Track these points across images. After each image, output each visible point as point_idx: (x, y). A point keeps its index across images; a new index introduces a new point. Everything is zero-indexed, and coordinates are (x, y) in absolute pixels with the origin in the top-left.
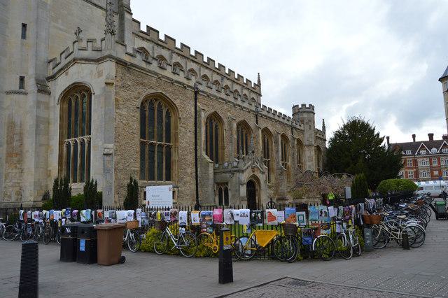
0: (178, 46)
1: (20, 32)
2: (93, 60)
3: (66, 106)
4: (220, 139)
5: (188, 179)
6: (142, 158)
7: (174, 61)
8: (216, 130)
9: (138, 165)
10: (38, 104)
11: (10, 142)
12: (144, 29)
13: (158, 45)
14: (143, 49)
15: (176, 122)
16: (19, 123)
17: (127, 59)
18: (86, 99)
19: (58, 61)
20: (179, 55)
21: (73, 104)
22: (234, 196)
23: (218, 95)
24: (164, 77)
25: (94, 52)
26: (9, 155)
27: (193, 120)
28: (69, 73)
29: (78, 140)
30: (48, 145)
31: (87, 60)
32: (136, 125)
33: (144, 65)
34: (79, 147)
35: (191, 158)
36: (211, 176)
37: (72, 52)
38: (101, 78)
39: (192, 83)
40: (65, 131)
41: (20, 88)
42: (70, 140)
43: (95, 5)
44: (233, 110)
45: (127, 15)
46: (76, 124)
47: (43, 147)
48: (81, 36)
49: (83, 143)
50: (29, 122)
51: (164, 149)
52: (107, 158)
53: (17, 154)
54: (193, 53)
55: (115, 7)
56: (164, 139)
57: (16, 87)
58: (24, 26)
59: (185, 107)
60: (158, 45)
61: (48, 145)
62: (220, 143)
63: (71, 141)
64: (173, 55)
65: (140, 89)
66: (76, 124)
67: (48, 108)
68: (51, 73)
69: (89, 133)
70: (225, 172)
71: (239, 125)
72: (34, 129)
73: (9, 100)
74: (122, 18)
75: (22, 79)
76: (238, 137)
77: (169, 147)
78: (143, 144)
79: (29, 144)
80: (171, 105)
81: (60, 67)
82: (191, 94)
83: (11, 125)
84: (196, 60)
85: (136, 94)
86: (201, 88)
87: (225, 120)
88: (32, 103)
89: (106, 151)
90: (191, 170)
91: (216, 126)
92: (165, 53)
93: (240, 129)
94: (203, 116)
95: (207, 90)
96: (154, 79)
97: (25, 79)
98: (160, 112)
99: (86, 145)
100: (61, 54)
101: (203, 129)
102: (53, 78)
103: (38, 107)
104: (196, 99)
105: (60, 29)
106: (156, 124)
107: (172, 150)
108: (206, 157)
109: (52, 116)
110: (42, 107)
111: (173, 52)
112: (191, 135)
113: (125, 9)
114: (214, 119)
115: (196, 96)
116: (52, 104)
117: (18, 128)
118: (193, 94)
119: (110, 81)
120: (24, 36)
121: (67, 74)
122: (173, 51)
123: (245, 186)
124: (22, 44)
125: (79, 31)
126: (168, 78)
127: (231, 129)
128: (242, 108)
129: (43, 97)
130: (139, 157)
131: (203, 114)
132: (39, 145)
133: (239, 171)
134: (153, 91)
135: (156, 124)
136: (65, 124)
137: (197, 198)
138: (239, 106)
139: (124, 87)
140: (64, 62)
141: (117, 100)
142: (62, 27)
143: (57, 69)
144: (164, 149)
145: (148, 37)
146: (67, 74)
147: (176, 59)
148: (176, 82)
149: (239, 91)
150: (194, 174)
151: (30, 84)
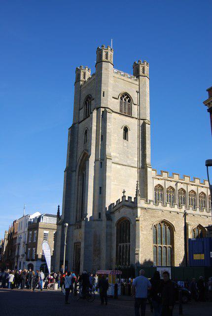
3: (119, 227)
10: (107, 226)
14: (159, 185)
23: (201, 213)
30: (111, 247)
31: (128, 206)
32: (151, 238)
33: (154, 207)
41: (100, 217)
42: (121, 244)
47: (109, 247)
49: (126, 246)
58: (101, 188)
84: (194, 184)
86: (188, 212)
96: (160, 213)
102: (113, 213)
103: (107, 228)
105: (115, 185)
110: (108, 227)
115: (185, 217)
125: (124, 192)
130: (152, 254)
131: (190, 228)
142: (117, 184)
145: (162, 178)
151: (104, 216)
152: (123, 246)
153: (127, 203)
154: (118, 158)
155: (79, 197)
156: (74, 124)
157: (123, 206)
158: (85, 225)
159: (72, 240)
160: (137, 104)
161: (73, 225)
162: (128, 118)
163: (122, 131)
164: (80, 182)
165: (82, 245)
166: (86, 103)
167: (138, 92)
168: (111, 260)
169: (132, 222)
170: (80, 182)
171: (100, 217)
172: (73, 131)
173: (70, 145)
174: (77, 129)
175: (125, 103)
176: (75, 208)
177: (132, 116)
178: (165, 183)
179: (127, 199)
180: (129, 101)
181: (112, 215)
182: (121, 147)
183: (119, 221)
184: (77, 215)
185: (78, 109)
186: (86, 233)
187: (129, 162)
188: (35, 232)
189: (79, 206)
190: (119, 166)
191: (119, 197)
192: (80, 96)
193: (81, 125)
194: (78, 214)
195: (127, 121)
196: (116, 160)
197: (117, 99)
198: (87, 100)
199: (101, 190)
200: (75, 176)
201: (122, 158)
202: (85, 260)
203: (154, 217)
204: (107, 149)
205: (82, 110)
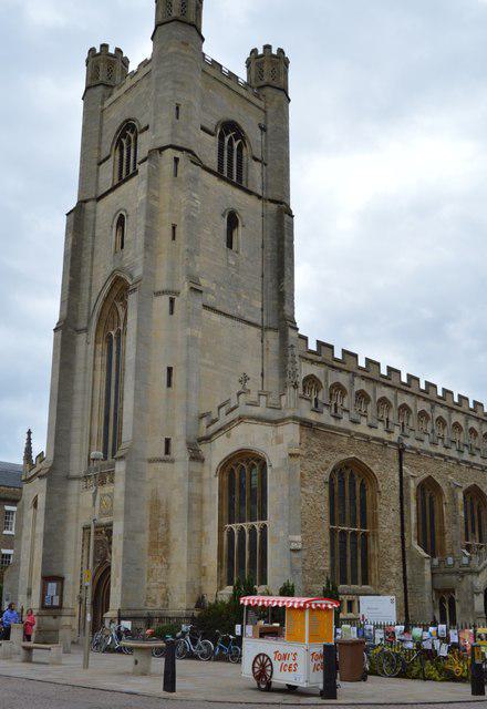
0: (362, 363)
1: (165, 378)
3: (226, 479)
4: (436, 517)
5: (392, 582)
6: (332, 554)
7: (357, 389)
8: (432, 503)
9: (328, 563)
10: (191, 475)
11: (154, 527)
12: (312, 346)
13: (333, 367)
15: (374, 499)
17: (312, 417)
18: (256, 471)
19: (214, 416)
20: (363, 378)
21: (237, 477)
22: (464, 611)
23: (432, 449)
24: (358, 434)
25: (269, 410)
26: (154, 545)
27: (397, 492)
29: (246, 526)
30: (202, 532)
31: (260, 419)
32: (324, 507)
33: (332, 422)
34: (247, 536)
35: (396, 551)
36: (428, 578)
37: (235, 408)
39: (394, 438)
40: (225, 513)
41: (167, 452)
43: (249, 323)
44: (456, 471)
45: (291, 333)
46: (242, 503)
47: (197, 535)
48: (249, 385)
50: (178, 501)
51: (359, 539)
52: (296, 555)
53: (163, 544)
54: (384, 371)
55: (270, 320)
57: (161, 453)
58: (170, 370)
59: (386, 472)
60: (333, 367)
61: (201, 531)
62: (437, 528)
63: (235, 527)
64: (357, 380)
65: (328, 456)
66: (242, 503)
67: (201, 481)
68: (204, 433)
69: (263, 516)
70: (451, 573)
71: (466, 493)
72: (186, 510)
73: (150, 471)
74: (284, 337)
75: (168, 442)
76: (466, 512)
77: (365, 535)
78: (332, 532)
79: (179, 530)
80: (367, 474)
81: (217, 425)
82: (393, 453)
83: (155, 504)
86: (408, 442)
87: (445, 488)
88: (182, 475)
89: (294, 546)
90: (396, 569)
91: (431, 498)
92: (343, 379)
93: (469, 499)
94: (413, 485)
95: (416, 444)
96: (345, 440)
97: (172, 442)
98: (353, 485)
99: (259, 535)
100: (219, 408)
101: (413, 506)
102: (208, 439)
104: (401, 460)
105: (208, 366)
106: (347, 501)
107: (370, 539)
108: (417, 547)
109: (206, 491)
111: (354, 375)
112: (395, 516)
114: (429, 488)
116: (206, 475)
117: (163, 508)
118: (396, 454)
119: (294, 451)
120: (169, 384)
121: (228, 436)
122: (355, 373)
123: (482, 596)
124: (168, 395)
125: (245, 379)
126: (363, 435)
127: (454, 502)
128: (471, 465)
129: (196, 467)
132: (192, 532)
133: (471, 572)
134: (343, 457)
135: (347, 501)
136: (225, 503)
137: (407, 611)
138: (466, 462)
139: (309, 456)
140: (224, 420)
141: (302, 475)
142: (210, 362)
143: (213, 428)
144: (359, 539)
145: (319, 359)
146: (228, 436)
147: (360, 385)
148: (374, 439)
149: (462, 424)
150: (401, 575)
151: (180, 450)
155: (96, 400)
156: (82, 203)
157: (241, 419)
158: (127, 473)
159: (77, 519)
160: (259, 157)
162: (238, 192)
163: (224, 222)
165: (118, 529)
166: (119, 144)
167: (263, 129)
168: (203, 573)
170: (99, 359)
171: (167, 452)
172: (78, 220)
173: (73, 260)
174: (92, 216)
176: (86, 430)
177: (250, 188)
178: (326, 374)
179: (253, 397)
180: (240, 148)
181: (203, 448)
185: (95, 161)
186: (128, 494)
187: (240, 310)
189: (96, 426)
190: (215, 318)
192: (101, 127)
193: (102, 205)
195: (236, 198)
196: (210, 299)
198: (124, 135)
200: (86, 346)
201: (224, 297)
202: (126, 573)
203: (331, 448)
205: (110, 163)
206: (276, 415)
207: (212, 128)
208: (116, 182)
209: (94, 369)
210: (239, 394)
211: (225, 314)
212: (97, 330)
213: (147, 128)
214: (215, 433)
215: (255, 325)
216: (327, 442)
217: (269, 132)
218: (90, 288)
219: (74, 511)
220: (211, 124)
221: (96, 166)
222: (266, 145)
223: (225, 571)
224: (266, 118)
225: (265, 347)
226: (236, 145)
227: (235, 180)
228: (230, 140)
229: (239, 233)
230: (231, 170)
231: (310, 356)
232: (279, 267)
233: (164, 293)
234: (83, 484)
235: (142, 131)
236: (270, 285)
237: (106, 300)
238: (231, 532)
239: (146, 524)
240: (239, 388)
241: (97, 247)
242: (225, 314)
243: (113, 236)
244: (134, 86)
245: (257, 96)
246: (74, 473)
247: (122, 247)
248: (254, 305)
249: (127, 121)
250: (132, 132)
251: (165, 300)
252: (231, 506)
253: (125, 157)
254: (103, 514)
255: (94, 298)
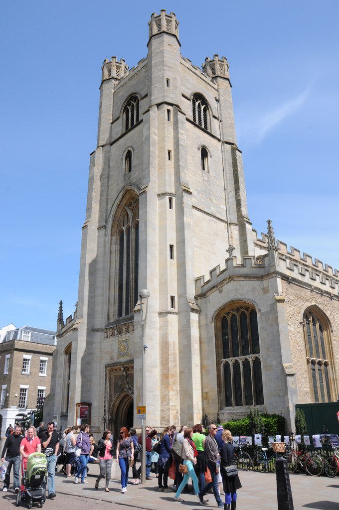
2: (254, 278)
3: (219, 324)
16: (172, 343)
17: (288, 273)
24: (316, 288)
28: (224, 291)
29: (240, 359)
31: (247, 277)
33: (300, 278)
38: (268, 295)
40: (221, 351)
43: (219, 219)
49: (246, 363)
53: (173, 375)
56: (321, 355)
63: (231, 361)
69: (255, 349)
81: (210, 285)
85: (297, 309)
99: (252, 365)
100: (211, 272)
113: (245, 219)
117: (171, 348)
121: (221, 292)
134: (309, 304)
136: (221, 343)
143: (206, 287)
146: (221, 292)
152: (236, 364)
153: (244, 271)
154: (196, 199)
157: (231, 278)
160: (217, 116)
161: (97, 330)
162: (206, 135)
163: (199, 154)
164: (114, 247)
166: (126, 110)
167: (218, 101)
169: (262, 308)
170: (114, 247)
175: (199, 112)
177: (213, 133)
180: (205, 110)
182: (200, 180)
183: (222, 309)
184: (109, 310)
188: (8, 356)
189: (112, 292)
191: (219, 261)
194: (112, 308)
197: (189, 100)
198: (129, 104)
199: (177, 251)
201: (203, 201)
204: (182, 174)
205: (120, 121)
206: (261, 272)
207: (188, 96)
208: (124, 131)
209: (111, 253)
210: (227, 261)
211: (204, 212)
212: (112, 227)
213: (146, 96)
214: (209, 290)
215: (223, 221)
216: (298, 293)
217: (221, 102)
218: (107, 200)
219: (98, 354)
220: (189, 94)
221: (110, 125)
222: (220, 110)
223: (223, 395)
224: (219, 95)
225: (230, 237)
226: (203, 107)
227: (203, 127)
228: (199, 104)
229: (209, 161)
230: (201, 123)
231: (259, 243)
232: (235, 183)
233: (165, 194)
234: (103, 334)
235: (143, 98)
236: (230, 195)
237: (118, 206)
238: (227, 364)
239: (158, 361)
240: (227, 256)
241: (111, 173)
242: (204, 212)
243: (124, 165)
244: (136, 74)
245: (213, 82)
246: (97, 327)
247: (130, 170)
248: (221, 206)
249: (131, 95)
250: (134, 101)
251: (167, 198)
252: (225, 344)
253: (130, 116)
254: (120, 355)
255: (110, 205)
